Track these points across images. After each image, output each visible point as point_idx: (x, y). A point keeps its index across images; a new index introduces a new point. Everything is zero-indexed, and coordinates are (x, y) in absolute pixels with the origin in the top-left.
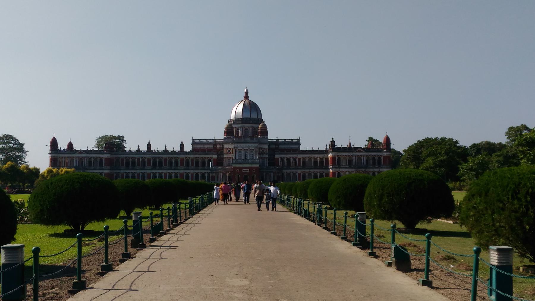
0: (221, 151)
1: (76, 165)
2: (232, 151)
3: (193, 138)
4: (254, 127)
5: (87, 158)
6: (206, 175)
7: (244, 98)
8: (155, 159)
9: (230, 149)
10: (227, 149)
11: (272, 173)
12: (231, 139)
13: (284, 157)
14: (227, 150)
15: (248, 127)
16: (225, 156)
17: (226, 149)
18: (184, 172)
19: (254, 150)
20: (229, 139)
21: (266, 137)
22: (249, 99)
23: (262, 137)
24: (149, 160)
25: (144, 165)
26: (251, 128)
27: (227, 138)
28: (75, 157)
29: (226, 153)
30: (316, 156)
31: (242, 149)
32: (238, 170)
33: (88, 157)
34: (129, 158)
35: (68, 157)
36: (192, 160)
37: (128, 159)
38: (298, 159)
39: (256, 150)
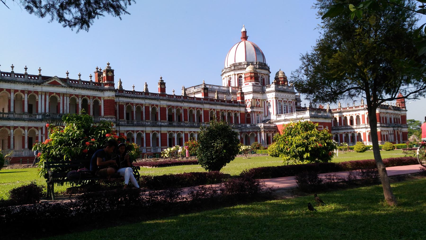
1: (43, 111)
2: (260, 103)
5: (68, 98)
8: (171, 108)
9: (259, 100)
12: (260, 86)
20: (257, 86)
24: (163, 110)
25: (156, 119)
27: (255, 84)
28: (42, 92)
29: (255, 105)
33: (71, 95)
34: (132, 104)
35: (23, 91)
37: (129, 106)
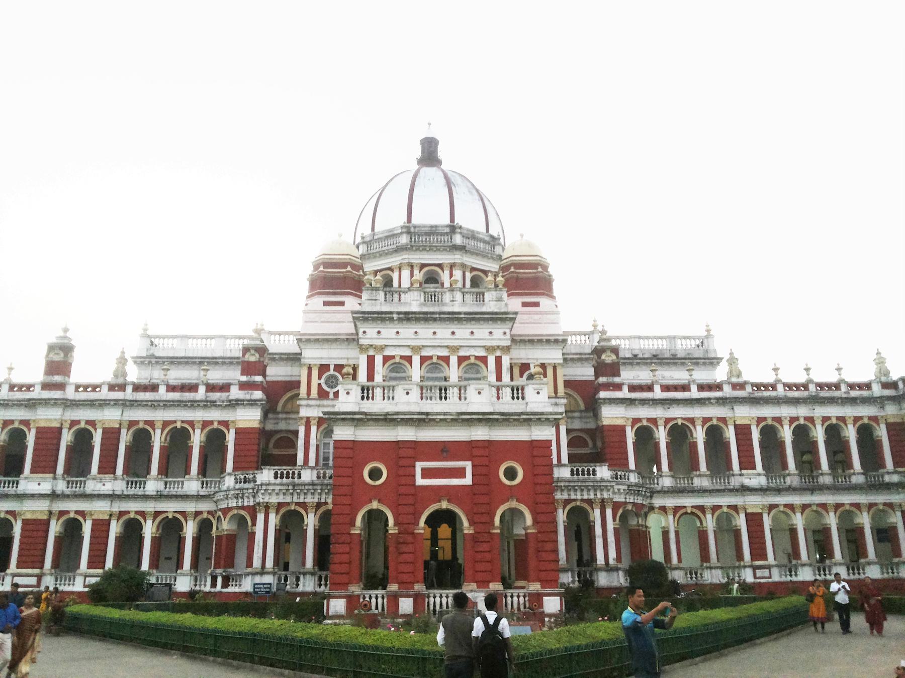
0: (289, 395)
3: (145, 330)
4: (473, 269)
6: (190, 530)
7: (417, 167)
10: (324, 368)
11: (609, 512)
13: (654, 421)
14: (320, 378)
15: (440, 266)
16: (304, 413)
17: (315, 373)
18: (50, 513)
19: (484, 360)
21: (544, 301)
22: (444, 166)
23: (525, 304)
26: (458, 274)
30: (833, 411)
31: (407, 353)
32: (375, 474)
36: (111, 436)
38: (736, 427)
39: (498, 360)
